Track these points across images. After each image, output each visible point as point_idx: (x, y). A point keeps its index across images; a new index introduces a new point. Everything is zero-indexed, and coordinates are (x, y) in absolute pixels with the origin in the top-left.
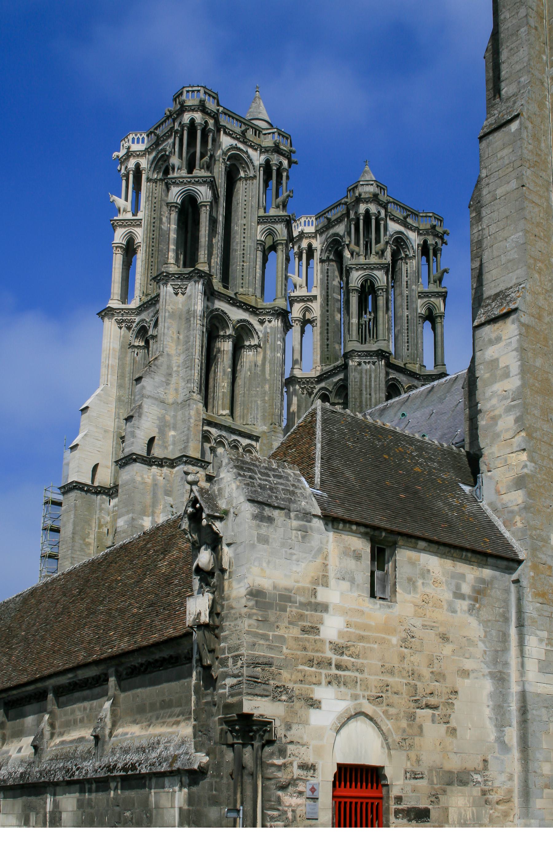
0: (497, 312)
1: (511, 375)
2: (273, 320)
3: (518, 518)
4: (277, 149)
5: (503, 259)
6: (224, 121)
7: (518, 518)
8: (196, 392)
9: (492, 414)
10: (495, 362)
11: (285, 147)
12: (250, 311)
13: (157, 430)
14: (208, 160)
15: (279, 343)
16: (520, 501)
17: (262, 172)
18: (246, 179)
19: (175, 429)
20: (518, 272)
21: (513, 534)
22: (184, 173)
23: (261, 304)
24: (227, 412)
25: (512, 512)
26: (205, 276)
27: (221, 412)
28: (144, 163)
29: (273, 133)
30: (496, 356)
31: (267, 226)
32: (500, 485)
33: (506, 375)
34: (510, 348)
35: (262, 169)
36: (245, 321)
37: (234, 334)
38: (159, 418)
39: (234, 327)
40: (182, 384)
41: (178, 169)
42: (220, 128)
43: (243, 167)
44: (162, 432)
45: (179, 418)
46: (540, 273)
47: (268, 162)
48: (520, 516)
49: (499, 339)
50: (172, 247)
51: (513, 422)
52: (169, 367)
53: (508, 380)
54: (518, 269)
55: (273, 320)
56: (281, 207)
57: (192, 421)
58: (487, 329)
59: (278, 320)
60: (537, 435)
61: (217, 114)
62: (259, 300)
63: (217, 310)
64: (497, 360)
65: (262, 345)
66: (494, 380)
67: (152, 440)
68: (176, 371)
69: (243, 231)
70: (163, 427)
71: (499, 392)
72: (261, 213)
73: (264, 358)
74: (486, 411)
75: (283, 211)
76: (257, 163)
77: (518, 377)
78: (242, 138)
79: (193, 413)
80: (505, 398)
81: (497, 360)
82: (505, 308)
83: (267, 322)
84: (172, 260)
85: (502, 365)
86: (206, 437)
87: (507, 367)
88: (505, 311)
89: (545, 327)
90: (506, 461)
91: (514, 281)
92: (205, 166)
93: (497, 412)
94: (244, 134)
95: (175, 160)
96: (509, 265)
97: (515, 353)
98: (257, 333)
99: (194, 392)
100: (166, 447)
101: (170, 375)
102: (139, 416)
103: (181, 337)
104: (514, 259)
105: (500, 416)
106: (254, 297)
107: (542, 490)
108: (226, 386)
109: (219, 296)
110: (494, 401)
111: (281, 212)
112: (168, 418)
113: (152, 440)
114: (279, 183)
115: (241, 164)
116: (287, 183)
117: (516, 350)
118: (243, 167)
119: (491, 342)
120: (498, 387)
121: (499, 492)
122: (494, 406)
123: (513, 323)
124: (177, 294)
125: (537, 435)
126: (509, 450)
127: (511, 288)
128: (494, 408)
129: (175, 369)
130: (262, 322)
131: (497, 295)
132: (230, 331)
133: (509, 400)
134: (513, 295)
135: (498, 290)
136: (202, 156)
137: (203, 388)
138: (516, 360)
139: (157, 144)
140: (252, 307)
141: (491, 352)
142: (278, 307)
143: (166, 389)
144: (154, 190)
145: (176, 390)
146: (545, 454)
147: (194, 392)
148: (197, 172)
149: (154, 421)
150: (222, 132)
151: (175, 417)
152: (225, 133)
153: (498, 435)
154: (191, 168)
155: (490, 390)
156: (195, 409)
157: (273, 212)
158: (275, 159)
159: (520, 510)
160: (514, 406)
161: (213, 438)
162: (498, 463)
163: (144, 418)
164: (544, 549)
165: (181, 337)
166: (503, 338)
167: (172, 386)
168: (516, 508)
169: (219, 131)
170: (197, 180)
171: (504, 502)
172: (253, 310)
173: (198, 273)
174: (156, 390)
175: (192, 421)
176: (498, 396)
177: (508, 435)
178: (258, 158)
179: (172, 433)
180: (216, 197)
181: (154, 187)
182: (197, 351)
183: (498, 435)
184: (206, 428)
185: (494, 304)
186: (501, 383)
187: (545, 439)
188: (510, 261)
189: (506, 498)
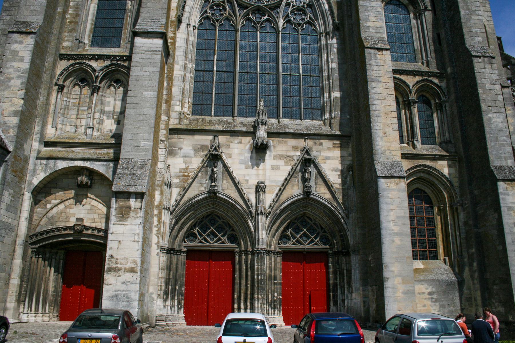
0: (24, 30)
1: (24, 61)
3: (11, 130)
5: (32, 8)
7: (11, 130)
9: (8, 76)
10: (15, 53)
16: (15, 122)
20: (39, 17)
21: (7, 137)
25: (9, 126)
30: (18, 49)
32: (4, 111)
33: (22, 60)
34: (27, 49)
46: (48, 23)
48: (13, 130)
49: (21, 42)
51: (20, 84)
53: (22, 63)
54: (39, 16)
58: (16, 35)
60: (29, 94)
64: (18, 52)
66: (13, 60)
71: (15, 67)
74: (4, 74)
77: (28, 64)
80: (18, 71)
81: (18, 52)
82: (28, 30)
85: (20, 54)
87: (23, 57)
88: (28, 31)
89: (44, 47)
90: (11, 101)
91: (35, 20)
93: (11, 76)
96: (34, 12)
97: (29, 52)
104: (38, 11)
105: (13, 78)
107: (26, 121)
110: (11, 70)
117: (30, 51)
119: (16, 42)
120: (15, 64)
121: (3, 115)
122: (10, 72)
123: (32, 38)
125: (29, 94)
126: (14, 96)
127: (33, 22)
128: (10, 73)
131: (24, 23)
133: (20, 73)
134: (34, 26)
135: (25, 20)
138: (29, 55)
141: (15, 47)
146: (31, 104)
153: (10, 87)
155: (10, 64)
159: (14, 127)
160: (22, 76)
162: (6, 100)
164: (21, 149)
166: (24, 43)
168: (12, 125)
171: (5, 120)
176: (14, 68)
177: (16, 89)
183: (10, 87)
185: (22, 26)
186: (17, 63)
187: (32, 97)
188: (35, 10)
189: (6, 119)
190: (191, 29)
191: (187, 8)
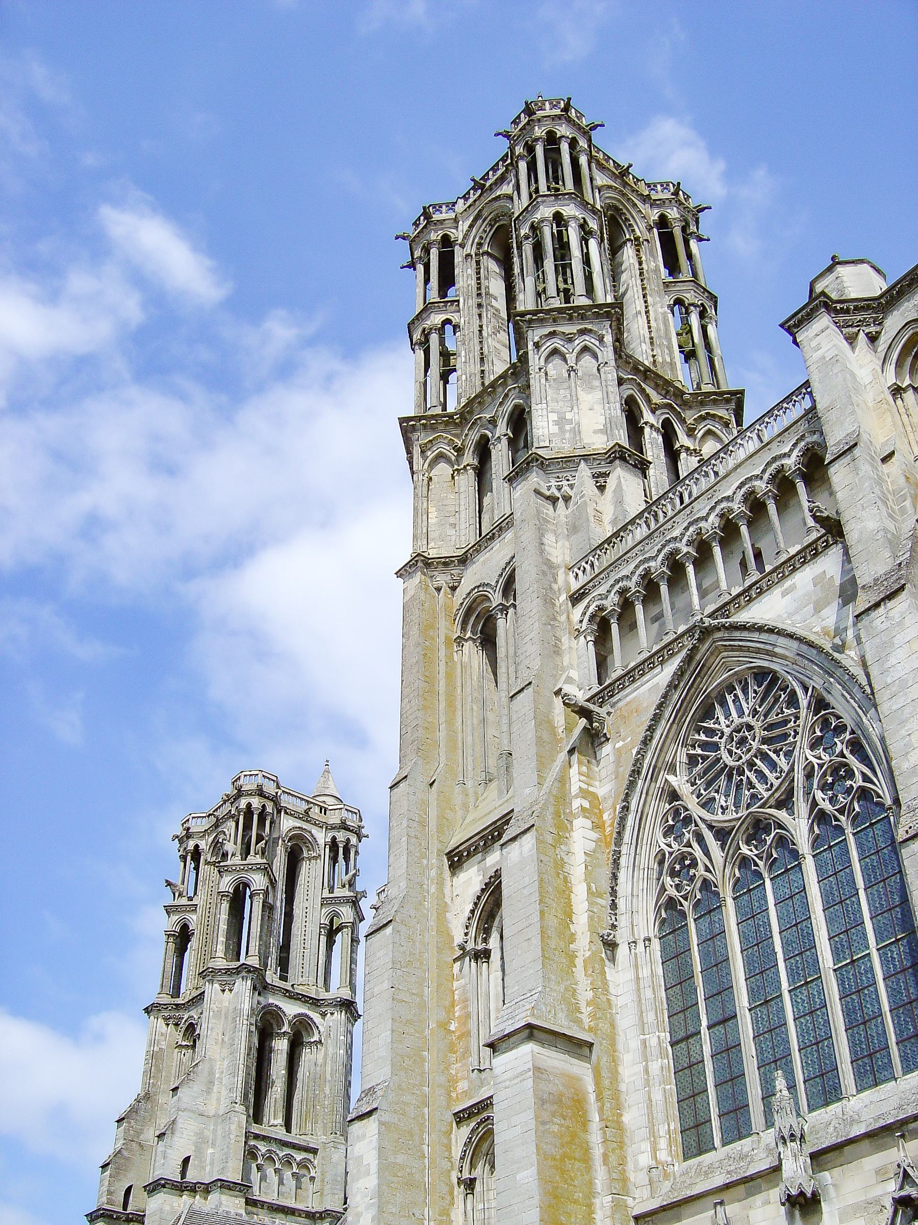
2: (336, 1013)
4: (344, 826)
6: (285, 801)
8: (239, 1103)
11: (353, 822)
12: (310, 1004)
13: (193, 1148)
14: (264, 846)
15: (342, 1038)
17: (327, 850)
18: (309, 859)
19: (213, 1145)
22: (237, 860)
23: (323, 995)
24: (280, 1121)
26: (253, 971)
27: (272, 1122)
28: (203, 845)
29: (341, 809)
31: (331, 908)
35: (327, 846)
36: (302, 1015)
37: (289, 1031)
38: (196, 1134)
39: (290, 1022)
40: (224, 1092)
41: (232, 855)
42: (281, 809)
43: (307, 847)
44: (199, 1150)
45: (219, 1132)
47: (334, 839)
50: (222, 939)
52: (211, 1073)
55: (336, 1013)
56: (347, 886)
57: (232, 1137)
59: (341, 1012)
61: (276, 797)
62: (320, 990)
63: (270, 1005)
65: (323, 1041)
67: (186, 1160)
68: (218, 1078)
69: (304, 914)
70: (201, 1141)
72: (326, 894)
73: (326, 1055)
75: (350, 891)
76: (321, 842)
78: (305, 816)
79: (233, 1127)
83: (329, 1014)
84: (220, 953)
86: (251, 1154)
92: (260, 852)
94: (308, 813)
95: (229, 847)
98: (318, 1027)
99: (236, 1103)
100: (204, 1168)
101: (211, 1082)
102: (172, 1133)
103: (226, 1039)
106: (315, 987)
108: (279, 1091)
109: (273, 989)
111: (347, 892)
112: (206, 1133)
113: (186, 1160)
114: (347, 858)
115: (305, 843)
116: (355, 859)
118: (307, 847)
124: (223, 991)
129: (217, 1076)
130: (324, 1015)
132: (286, 1028)
136: (260, 838)
137: (251, 1097)
139: (216, 825)
140: (311, 998)
142: (341, 998)
143: (206, 1099)
144: (212, 873)
145: (218, 1099)
147: (236, 1103)
148: (251, 859)
149: (190, 1138)
150: (282, 813)
151: (215, 1131)
152: (286, 813)
154: (246, 852)
156: (236, 1123)
157: (338, 892)
158: (341, 836)
161: (260, 1153)
163: (177, 1134)
165: (226, 1039)
167: (214, 1095)
169: (279, 812)
170: (250, 867)
172: (315, 1003)
173: (246, 968)
174: (195, 1101)
175: (232, 1137)
178: (322, 837)
179: (210, 1151)
180: (273, 883)
181: (212, 870)
182: (242, 1055)
184: (252, 1143)
190: (641, 946)
191: (621, 903)
